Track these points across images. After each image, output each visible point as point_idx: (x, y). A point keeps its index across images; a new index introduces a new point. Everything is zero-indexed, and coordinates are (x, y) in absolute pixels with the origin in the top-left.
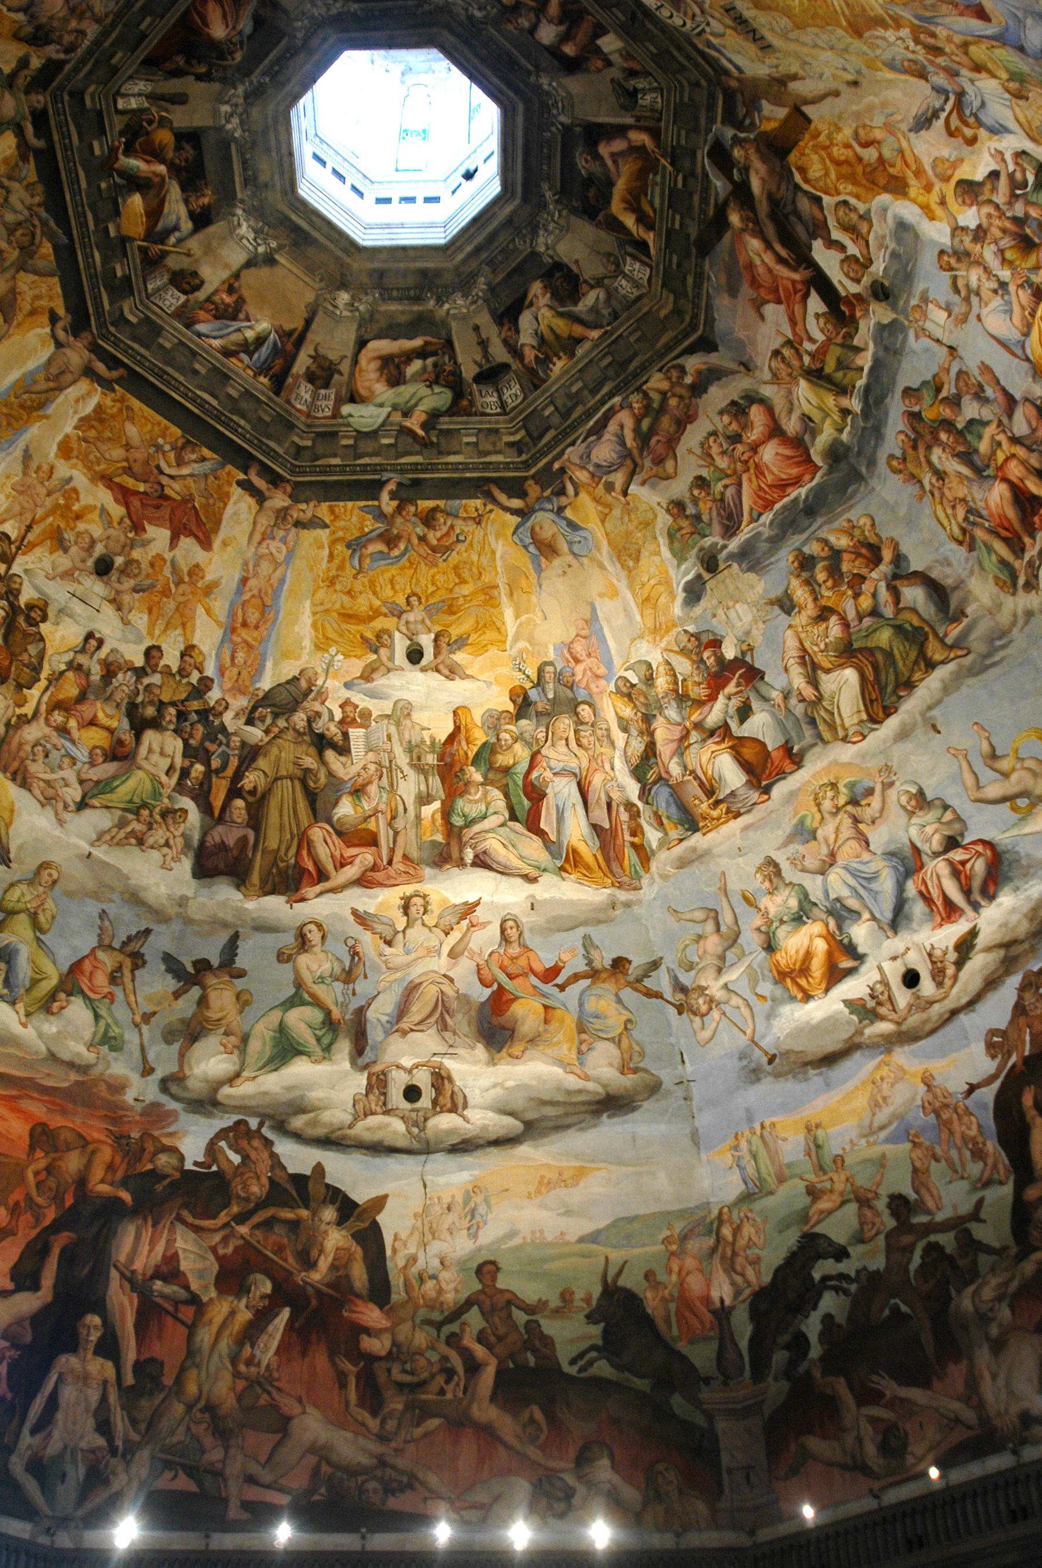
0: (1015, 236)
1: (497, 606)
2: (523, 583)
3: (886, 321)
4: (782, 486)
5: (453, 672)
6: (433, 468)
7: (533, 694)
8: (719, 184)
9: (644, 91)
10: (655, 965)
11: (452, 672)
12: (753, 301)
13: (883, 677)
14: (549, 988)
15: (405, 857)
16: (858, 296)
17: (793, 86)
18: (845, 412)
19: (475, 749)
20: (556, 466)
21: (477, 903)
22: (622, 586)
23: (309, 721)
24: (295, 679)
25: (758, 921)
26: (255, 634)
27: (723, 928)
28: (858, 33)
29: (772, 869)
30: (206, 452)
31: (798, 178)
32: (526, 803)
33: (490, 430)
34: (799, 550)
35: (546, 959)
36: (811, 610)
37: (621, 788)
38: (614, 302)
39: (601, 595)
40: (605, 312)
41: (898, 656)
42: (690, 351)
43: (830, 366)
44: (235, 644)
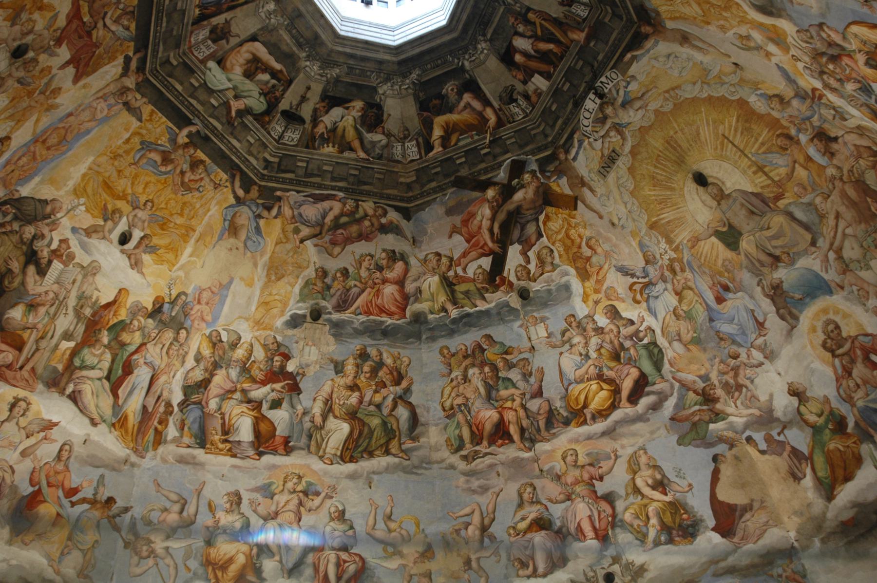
0: (614, 348)
1: (186, 242)
2: (208, 239)
3: (512, 305)
4: (382, 310)
5: (136, 264)
6: (221, 137)
7: (166, 307)
8: (502, 174)
9: (519, 106)
10: (126, 510)
11: (136, 264)
12: (455, 226)
13: (361, 441)
14: (66, 502)
15: (33, 369)
16: (511, 285)
17: (586, 191)
18: (444, 309)
19: (116, 321)
20: (278, 193)
21: (56, 424)
22: (258, 285)
23: (35, 237)
24: (46, 202)
25: (210, 522)
26: (44, 152)
27: (185, 514)
28: (653, 226)
29: (236, 499)
30: (133, 26)
31: (542, 217)
32: (120, 372)
33: (264, 144)
34: (365, 347)
35: (74, 481)
36: (349, 380)
37: (171, 392)
38: (386, 151)
39: (242, 279)
40: (377, 151)
41: (375, 436)
42: (397, 209)
43: (461, 288)
44: (29, 151)
